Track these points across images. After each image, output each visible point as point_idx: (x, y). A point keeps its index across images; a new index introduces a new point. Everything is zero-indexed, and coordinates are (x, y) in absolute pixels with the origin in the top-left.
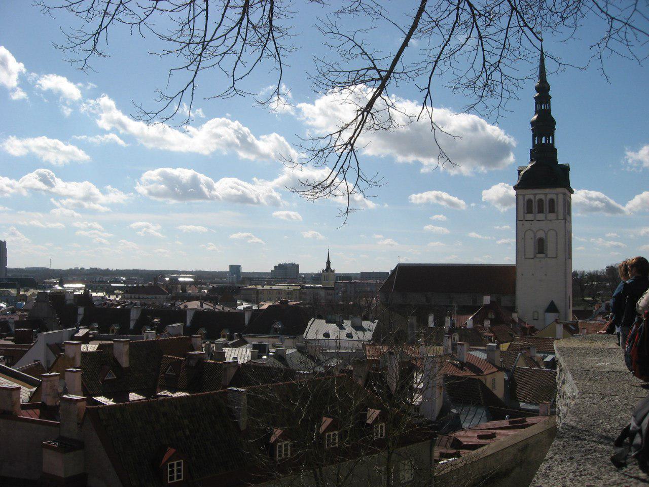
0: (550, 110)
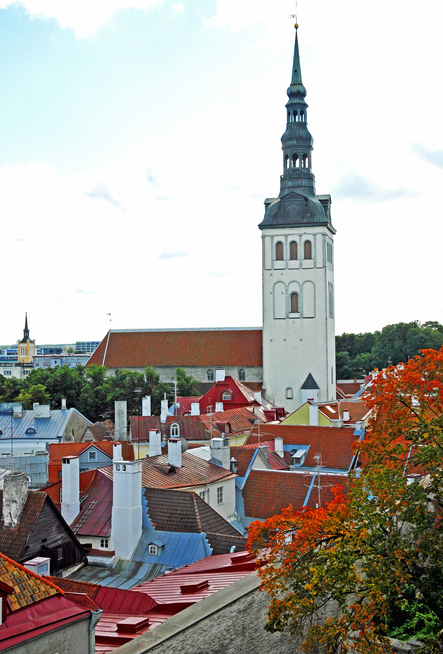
0: (305, 123)
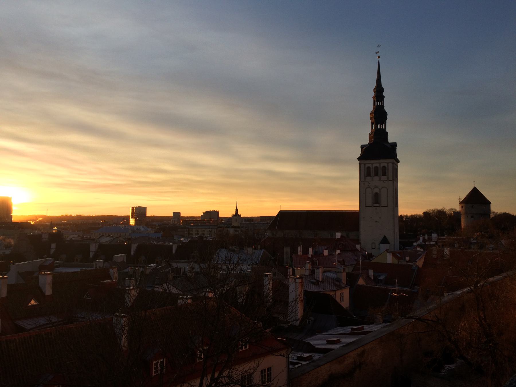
0: (383, 106)
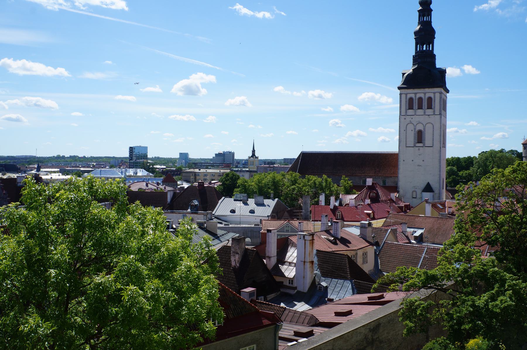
0: (430, 22)
